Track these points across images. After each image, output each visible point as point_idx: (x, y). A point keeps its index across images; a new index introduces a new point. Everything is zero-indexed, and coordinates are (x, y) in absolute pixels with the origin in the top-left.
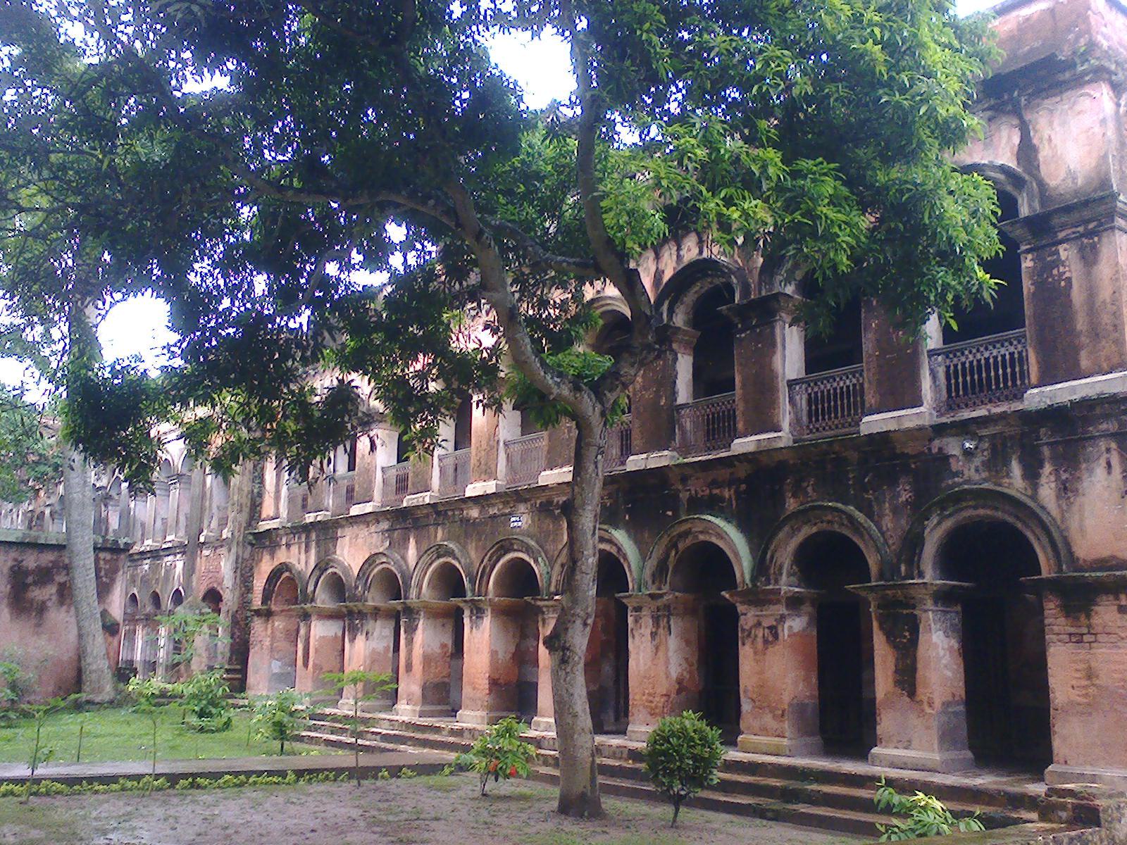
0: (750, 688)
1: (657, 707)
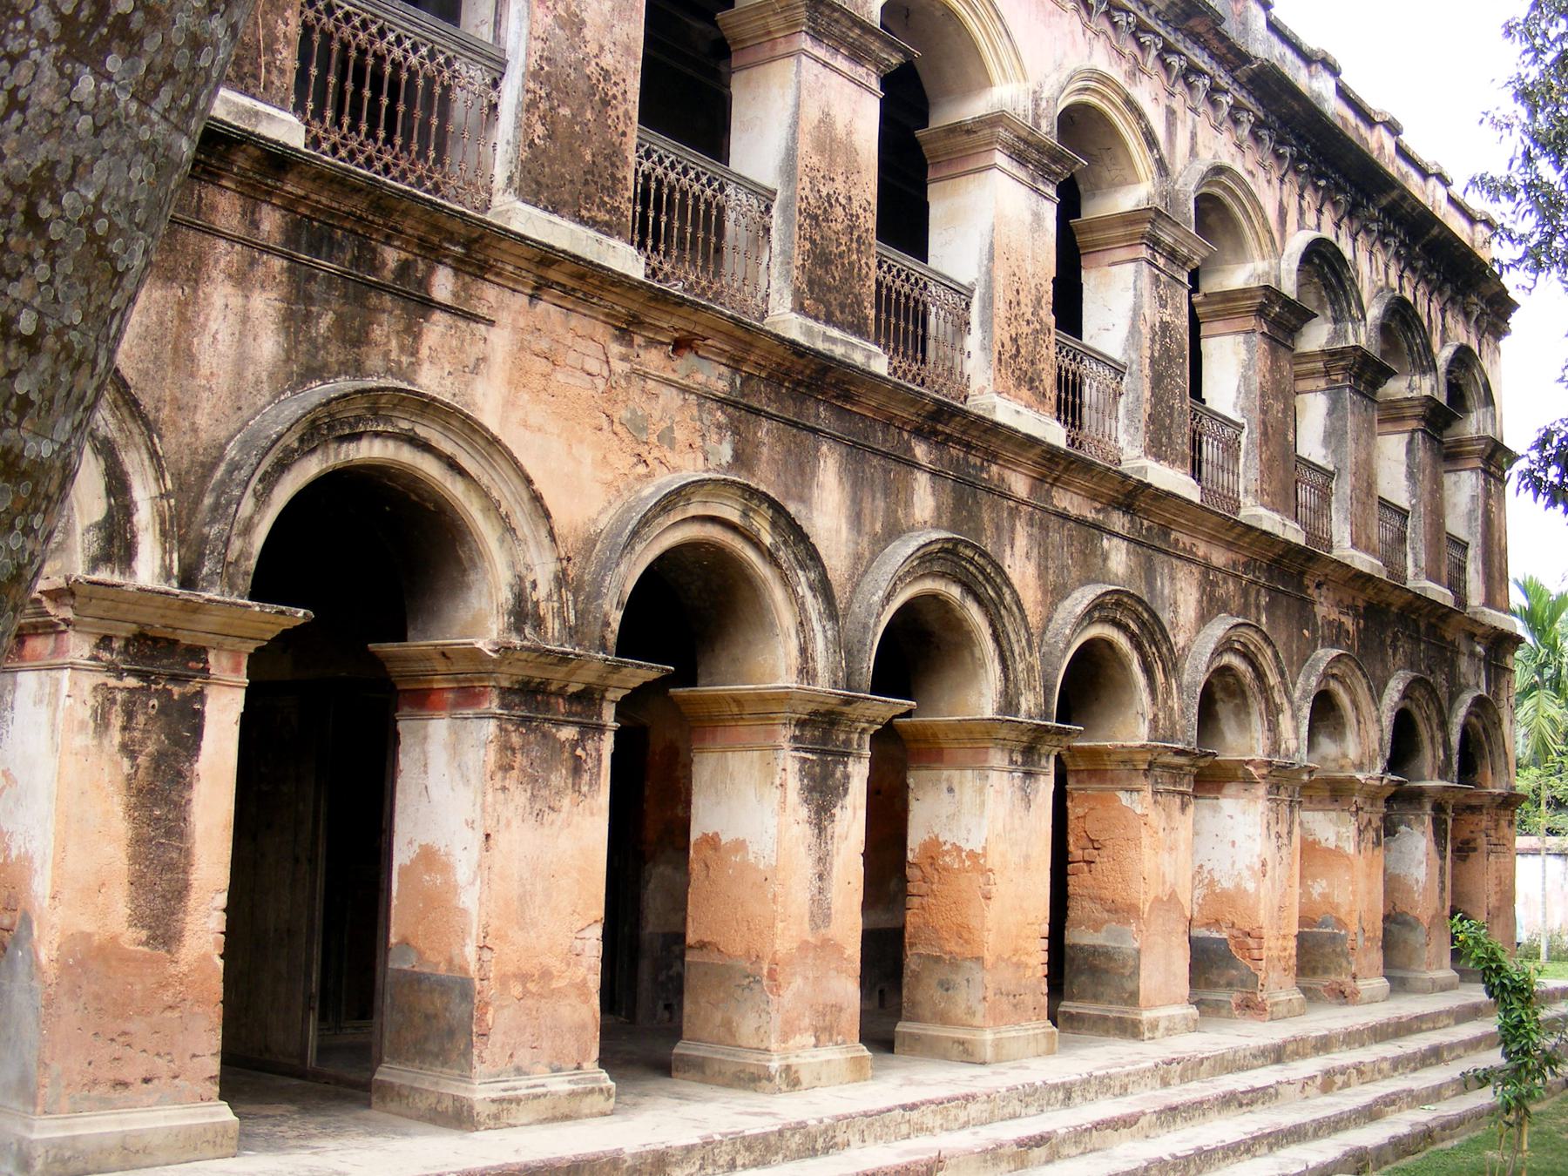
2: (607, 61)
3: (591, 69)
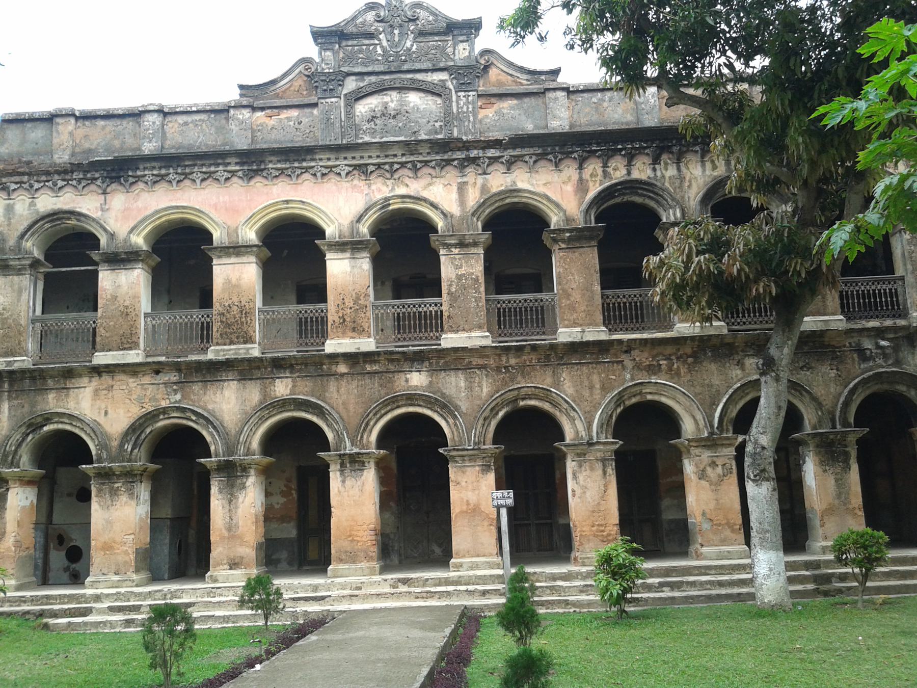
0: (707, 511)
1: (609, 535)
2: (127, 303)
3: (122, 308)
